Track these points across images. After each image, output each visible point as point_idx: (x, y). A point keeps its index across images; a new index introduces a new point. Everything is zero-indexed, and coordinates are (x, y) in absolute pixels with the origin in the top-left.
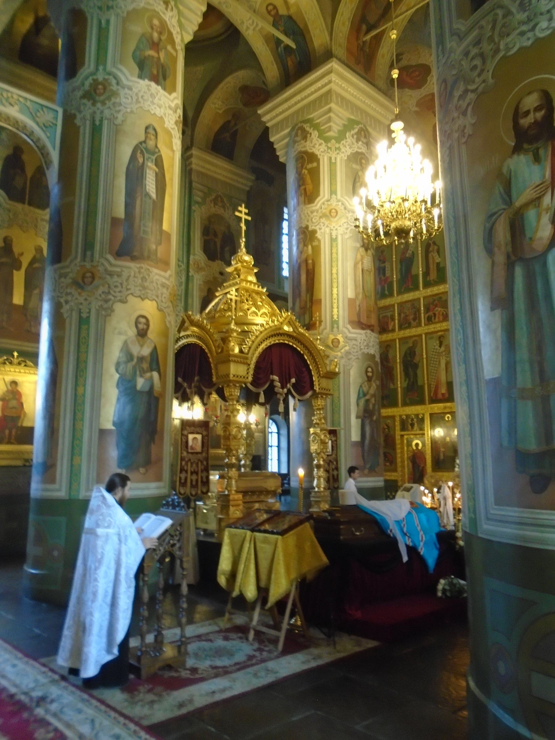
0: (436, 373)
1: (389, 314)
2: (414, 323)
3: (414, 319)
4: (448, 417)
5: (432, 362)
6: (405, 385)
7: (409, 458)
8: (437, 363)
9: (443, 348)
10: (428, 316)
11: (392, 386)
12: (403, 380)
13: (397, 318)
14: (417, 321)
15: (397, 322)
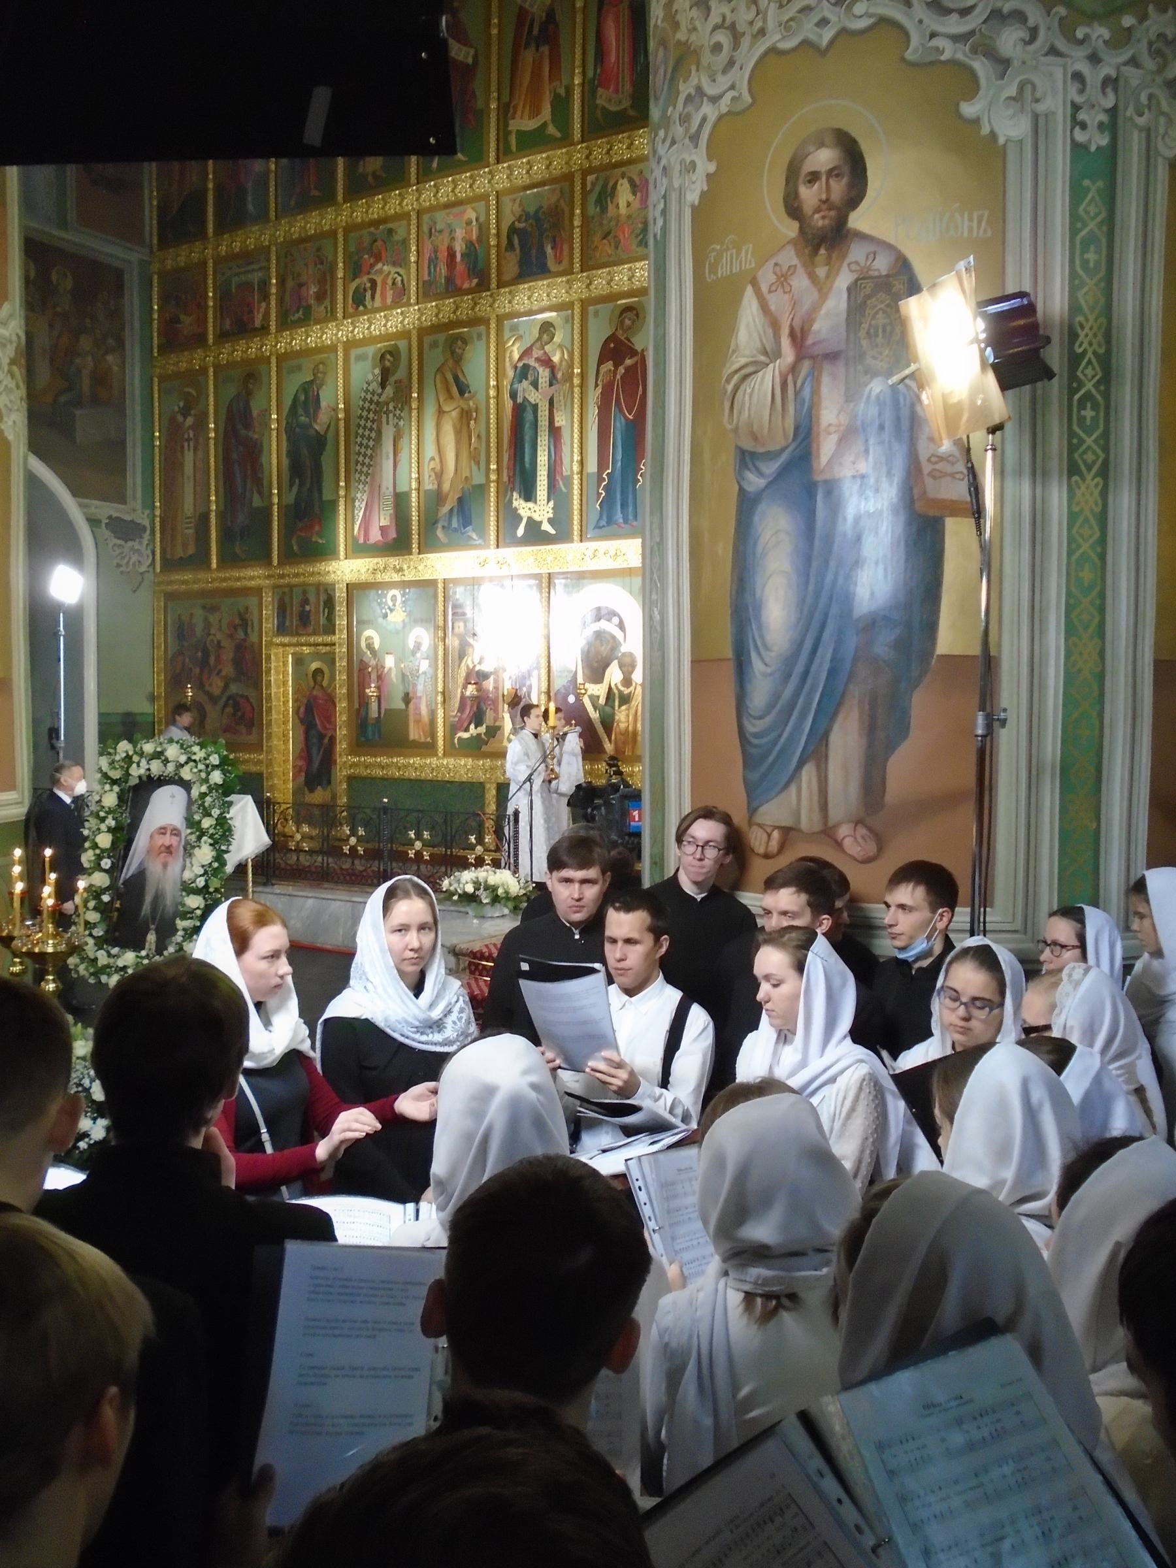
0: (369, 466)
1: (256, 277)
2: (320, 310)
3: (320, 297)
4: (394, 598)
5: (360, 431)
6: (290, 498)
7: (296, 712)
8: (373, 435)
9: (389, 391)
10: (357, 289)
11: (257, 502)
12: (285, 484)
13: (274, 290)
14: (327, 302)
15: (273, 303)
